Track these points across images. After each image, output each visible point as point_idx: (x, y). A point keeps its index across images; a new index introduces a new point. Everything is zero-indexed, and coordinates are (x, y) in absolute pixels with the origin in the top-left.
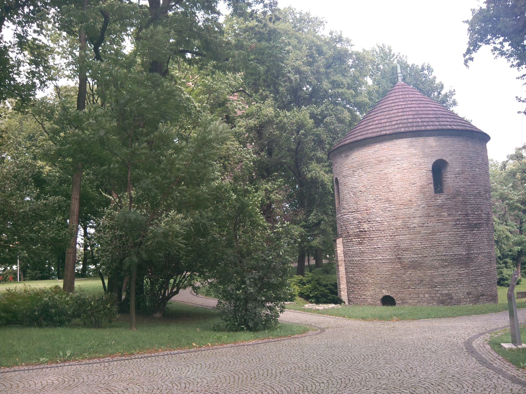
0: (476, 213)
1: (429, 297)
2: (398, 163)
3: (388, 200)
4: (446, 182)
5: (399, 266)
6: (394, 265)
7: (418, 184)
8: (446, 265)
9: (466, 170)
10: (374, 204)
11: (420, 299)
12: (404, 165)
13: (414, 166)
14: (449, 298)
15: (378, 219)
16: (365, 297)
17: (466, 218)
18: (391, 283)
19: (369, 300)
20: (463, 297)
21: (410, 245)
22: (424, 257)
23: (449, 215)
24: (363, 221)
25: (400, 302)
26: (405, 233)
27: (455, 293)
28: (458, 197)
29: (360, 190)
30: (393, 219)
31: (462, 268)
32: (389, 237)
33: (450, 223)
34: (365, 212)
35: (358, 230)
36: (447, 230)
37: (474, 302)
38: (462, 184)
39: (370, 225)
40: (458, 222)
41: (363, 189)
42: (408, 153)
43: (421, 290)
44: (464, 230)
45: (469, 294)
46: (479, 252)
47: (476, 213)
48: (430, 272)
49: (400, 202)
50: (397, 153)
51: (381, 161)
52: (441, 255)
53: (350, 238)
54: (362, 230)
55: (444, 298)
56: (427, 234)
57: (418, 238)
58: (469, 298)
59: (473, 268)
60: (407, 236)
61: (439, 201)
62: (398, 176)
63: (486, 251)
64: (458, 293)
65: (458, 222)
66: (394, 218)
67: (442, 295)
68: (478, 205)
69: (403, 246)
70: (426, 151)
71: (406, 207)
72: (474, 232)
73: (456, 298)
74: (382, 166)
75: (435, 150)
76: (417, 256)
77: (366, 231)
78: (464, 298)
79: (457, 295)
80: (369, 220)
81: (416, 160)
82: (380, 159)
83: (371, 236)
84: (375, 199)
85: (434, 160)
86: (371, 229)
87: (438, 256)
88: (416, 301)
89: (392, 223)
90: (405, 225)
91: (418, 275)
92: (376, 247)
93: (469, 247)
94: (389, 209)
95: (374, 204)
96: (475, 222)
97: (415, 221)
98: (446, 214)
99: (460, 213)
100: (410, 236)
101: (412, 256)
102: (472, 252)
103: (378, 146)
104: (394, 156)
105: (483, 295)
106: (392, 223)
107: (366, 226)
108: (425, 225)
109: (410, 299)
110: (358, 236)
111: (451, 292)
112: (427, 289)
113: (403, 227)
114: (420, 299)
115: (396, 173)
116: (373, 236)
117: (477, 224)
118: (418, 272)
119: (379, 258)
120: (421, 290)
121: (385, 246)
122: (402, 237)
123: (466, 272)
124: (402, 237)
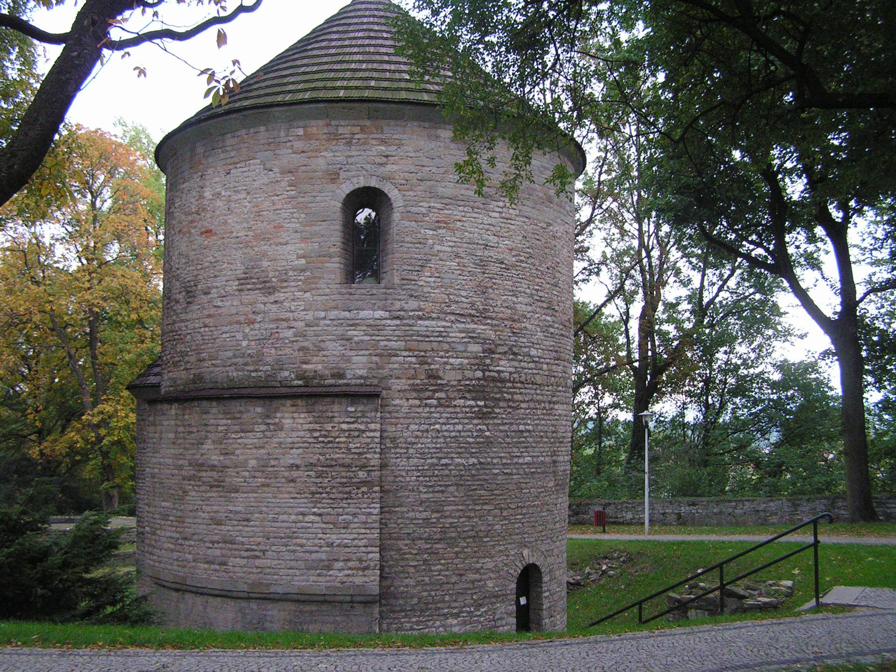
10: (530, 309)
15: (533, 352)
16: (477, 576)
18: (540, 528)
19: (490, 584)
29: (501, 256)
34: (508, 323)
35: (479, 374)
39: (516, 364)
41: (511, 260)
54: (496, 375)
77: (502, 381)
80: (515, 350)
83: (516, 397)
84: (531, 296)
92: (522, 427)
95: (530, 309)
107: (505, 366)
110: (477, 392)
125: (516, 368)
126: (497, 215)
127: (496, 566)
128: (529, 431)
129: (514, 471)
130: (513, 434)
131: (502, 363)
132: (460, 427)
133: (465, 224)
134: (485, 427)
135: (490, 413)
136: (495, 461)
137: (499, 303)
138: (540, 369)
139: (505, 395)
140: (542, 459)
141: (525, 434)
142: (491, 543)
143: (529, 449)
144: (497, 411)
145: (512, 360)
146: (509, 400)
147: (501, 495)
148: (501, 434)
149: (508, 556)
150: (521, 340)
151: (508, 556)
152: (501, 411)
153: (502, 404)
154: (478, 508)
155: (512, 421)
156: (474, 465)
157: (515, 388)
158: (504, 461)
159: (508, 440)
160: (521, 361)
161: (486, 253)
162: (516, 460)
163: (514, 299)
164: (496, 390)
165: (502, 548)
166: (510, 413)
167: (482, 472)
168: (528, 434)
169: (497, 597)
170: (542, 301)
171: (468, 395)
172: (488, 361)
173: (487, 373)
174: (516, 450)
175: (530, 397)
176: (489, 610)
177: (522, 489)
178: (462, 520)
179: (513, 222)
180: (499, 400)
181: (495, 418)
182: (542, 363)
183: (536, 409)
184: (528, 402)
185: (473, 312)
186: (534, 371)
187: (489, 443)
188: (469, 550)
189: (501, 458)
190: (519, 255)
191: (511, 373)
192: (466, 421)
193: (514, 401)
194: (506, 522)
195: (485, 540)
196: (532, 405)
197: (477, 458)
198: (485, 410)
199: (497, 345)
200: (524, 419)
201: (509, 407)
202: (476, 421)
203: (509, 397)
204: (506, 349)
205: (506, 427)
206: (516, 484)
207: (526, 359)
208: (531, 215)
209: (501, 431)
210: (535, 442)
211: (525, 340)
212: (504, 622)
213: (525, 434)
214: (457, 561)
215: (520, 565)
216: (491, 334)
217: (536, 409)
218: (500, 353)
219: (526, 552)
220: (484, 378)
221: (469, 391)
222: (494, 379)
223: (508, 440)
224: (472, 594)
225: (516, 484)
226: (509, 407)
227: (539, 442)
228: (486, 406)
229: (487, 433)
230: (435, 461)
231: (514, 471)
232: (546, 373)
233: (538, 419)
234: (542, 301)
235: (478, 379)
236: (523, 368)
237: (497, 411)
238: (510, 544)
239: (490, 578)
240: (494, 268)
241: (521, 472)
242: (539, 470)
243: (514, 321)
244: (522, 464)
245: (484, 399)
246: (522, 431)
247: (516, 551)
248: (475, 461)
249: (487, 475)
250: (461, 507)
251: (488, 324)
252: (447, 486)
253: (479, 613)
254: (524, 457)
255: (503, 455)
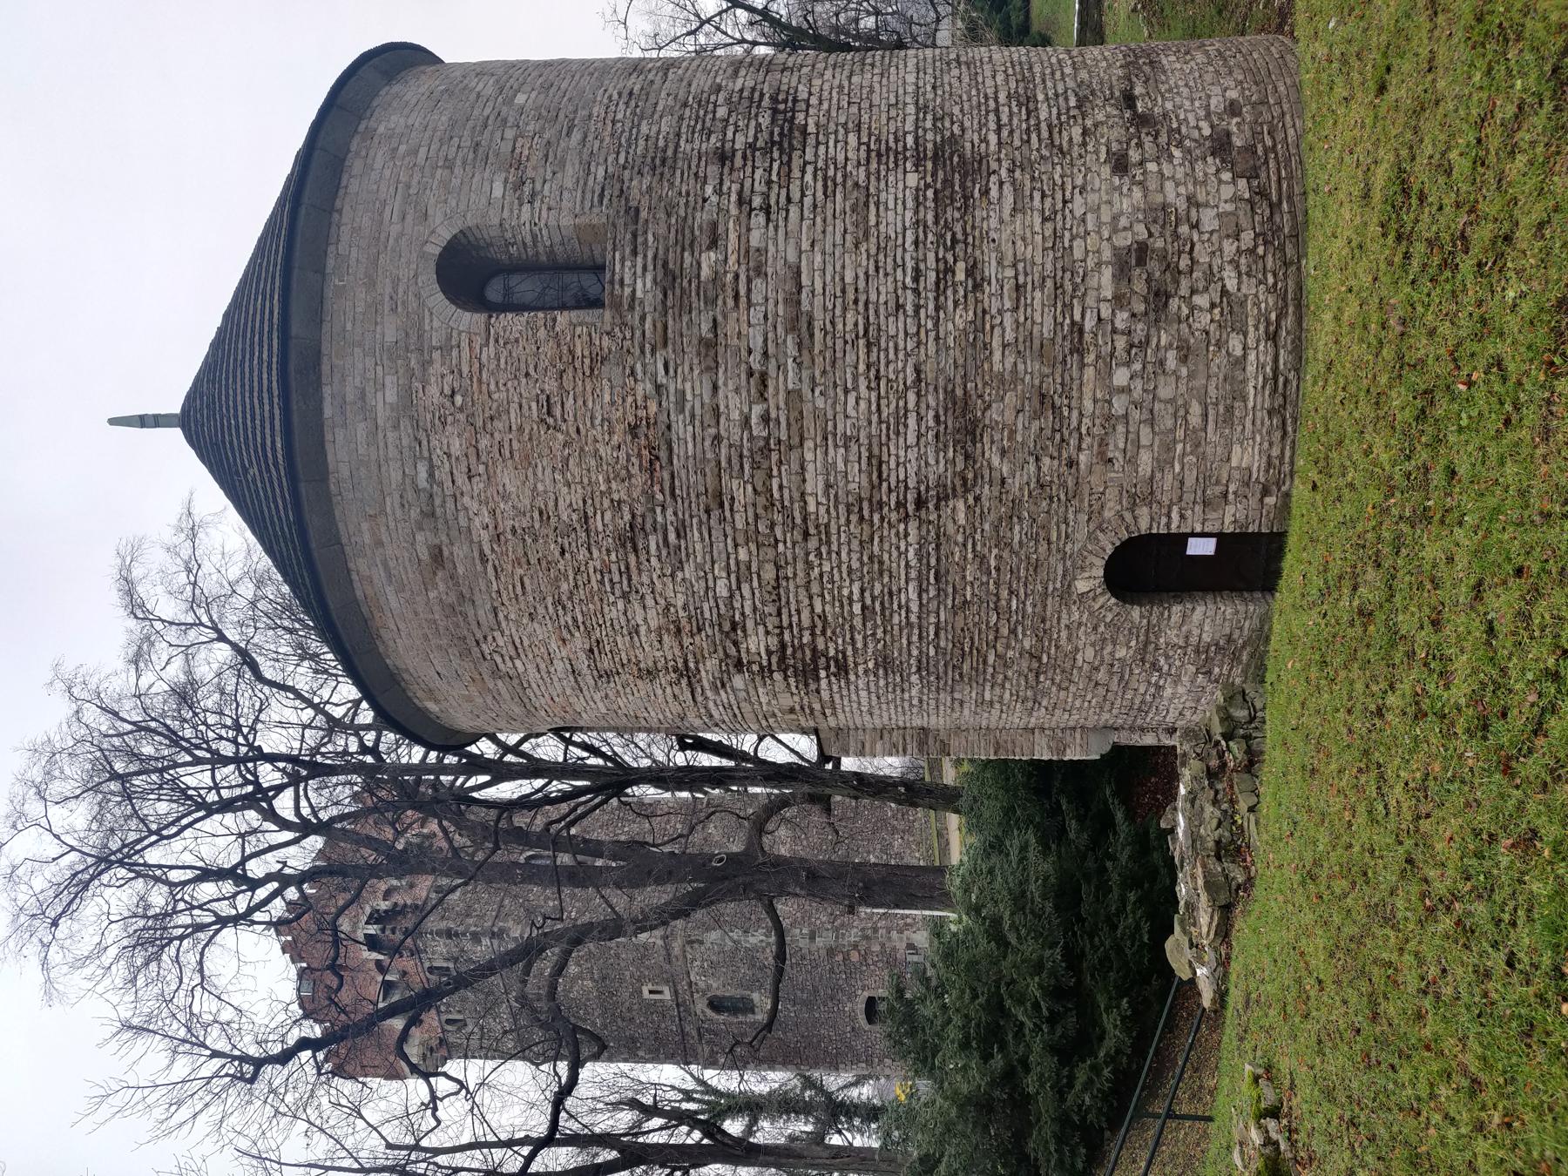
0: (722, 112)
1: (1128, 364)
2: (442, 474)
3: (630, 539)
4: (558, 249)
5: (961, 505)
6: (951, 529)
7: (551, 386)
8: (970, 273)
9: (506, 148)
10: (650, 602)
11: (1136, 415)
12: (456, 447)
13: (458, 399)
14: (1141, 262)
15: (722, 590)
17: (738, 162)
18: (1043, 548)
19: (1121, 653)
20: (1137, 193)
21: (854, 448)
22: (918, 380)
23: (713, 244)
24: (732, 651)
25: (1144, 512)
26: (795, 467)
27: (1115, 230)
28: (635, 193)
30: (722, 520)
31: (986, 192)
32: (813, 543)
33: (755, 239)
34: (687, 641)
35: (777, 676)
36: (792, 258)
37: (1163, 139)
38: (569, 170)
39: (750, 624)
40: (757, 201)
41: (579, 642)
42: (396, 427)
43: (1088, 404)
44: (796, 173)
45: (1120, 165)
46: (911, 109)
47: (722, 112)
48: (997, 356)
49: (639, 480)
50: (396, 476)
51: (438, 556)
52: (916, 291)
53: (817, 706)
54: (774, 659)
55: (1140, 286)
56: (806, 357)
57: (820, 403)
58: (1141, 163)
59: (993, 138)
60: (809, 456)
61: (644, 287)
62: (508, 478)
63: (911, 79)
64: (1115, 218)
65: (757, 201)
66: (715, 514)
67: (1119, 301)
68: (685, 105)
69: (858, 480)
70: (390, 337)
71: (663, 455)
72: (811, 129)
73: (1140, 229)
74: (460, 551)
75: (388, 290)
76: (912, 421)
77: (783, 646)
78: (1145, 190)
79: (1123, 222)
80: (727, 627)
81: (433, 390)
82: (424, 555)
83: (806, 622)
84: (625, 596)
85: (438, 299)
86: (771, 622)
87: (917, 308)
88: (1145, 431)
89: (740, 525)
90: (756, 466)
91: (1009, 416)
92: (857, 608)
93: (883, 154)
94: (672, 537)
96: (765, 120)
97: (735, 415)
98: (709, 259)
99: (709, 190)
100: (809, 444)
101: (911, 439)
102: (910, 140)
103: (360, 565)
104: (410, 495)
105: (1129, 100)
106: (740, 525)
107: (756, 643)
108: (756, 367)
109: (1132, 461)
111: (1107, 254)
112: (1089, 372)
113: (760, 476)
114: (1136, 415)
115: (492, 491)
116: (805, 615)
117: (775, 111)
118: (994, 414)
119: (913, 595)
120: (1088, 404)
121: (856, 565)
122: (814, 484)
123: (1011, 171)
124: (814, 484)
125: (756, 624)
126: (518, 663)
127: (1093, 645)
128: (862, 591)
129: (932, 620)
130: (869, 625)
131: (753, 649)
132: (863, 694)
133: (554, 694)
134: (861, 669)
135: (837, 661)
136: (915, 652)
137: (658, 654)
138: (749, 568)
139: (805, 640)
140: (911, 554)
141: (868, 601)
142: (1053, 651)
143: (894, 589)
144: (832, 653)
145: (744, 631)
146: (813, 634)
147: (972, 639)
148: (871, 646)
149: (1080, 624)
150: (707, 615)
151: (1080, 624)
152: (831, 645)
153: (821, 646)
154: (990, 670)
155: (847, 627)
156: (921, 678)
157: (791, 625)
158: (915, 638)
159: (880, 632)
160: (743, 614)
161: (585, 671)
162: (913, 619)
163: (643, 630)
164: (799, 655)
165: (1064, 634)
166: (834, 633)
167: (932, 669)
168: (867, 594)
169: (1147, 643)
170: (628, 568)
171: (813, 686)
172: (755, 668)
173: (774, 667)
174: (896, 620)
175: (802, 592)
176: (1167, 657)
177: (965, 602)
178: (1007, 685)
179: (518, 641)
180: (814, 650)
181: (844, 653)
182: (738, 563)
183: (821, 575)
184: (811, 598)
185: (684, 682)
186: (755, 584)
187: (885, 663)
188: (1058, 679)
189: (909, 643)
190: (567, 626)
191: (767, 633)
192: (852, 687)
193: (813, 627)
194: (1020, 629)
195: (1045, 659)
196: (815, 588)
197: (909, 675)
198: (833, 669)
199: (727, 656)
200: (842, 606)
201: (824, 633)
202: (852, 677)
203: (807, 634)
204: (729, 644)
205: (859, 638)
206: (955, 614)
207: (737, 605)
208: (488, 606)
209: (865, 645)
210: (881, 574)
211: (706, 607)
212: (1196, 632)
213: (868, 601)
214: (1073, 689)
215: (1101, 600)
216: (711, 664)
217: (821, 575)
218: (739, 651)
219: (1082, 586)
220: (785, 671)
221: (806, 685)
222: (782, 659)
223: (880, 632)
224: (1131, 673)
225: (955, 614)
226: (824, 633)
227: (881, 563)
228: (827, 668)
229: (871, 665)
230: (915, 710)
231: (932, 620)
232: (753, 547)
233: (839, 567)
234: (628, 568)
235: (786, 678)
236: (755, 609)
237: (832, 653)
238: (1059, 619)
239: (1112, 654)
240: (606, 664)
241: (933, 606)
242: (933, 562)
243: (679, 631)
244: (921, 605)
245: (816, 670)
246: (864, 608)
247: (1074, 608)
248: (914, 678)
249: (938, 662)
250: (988, 688)
251: (697, 669)
252: (953, 699)
253: (1166, 668)
254: (908, 600)
255: (904, 641)
